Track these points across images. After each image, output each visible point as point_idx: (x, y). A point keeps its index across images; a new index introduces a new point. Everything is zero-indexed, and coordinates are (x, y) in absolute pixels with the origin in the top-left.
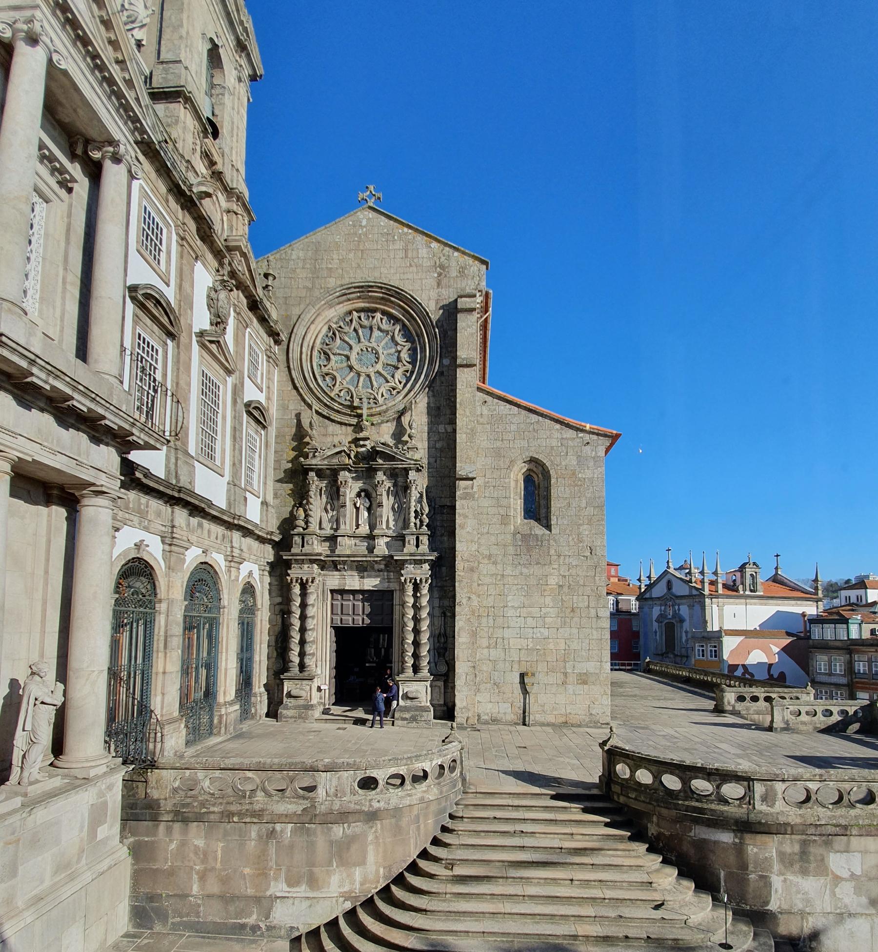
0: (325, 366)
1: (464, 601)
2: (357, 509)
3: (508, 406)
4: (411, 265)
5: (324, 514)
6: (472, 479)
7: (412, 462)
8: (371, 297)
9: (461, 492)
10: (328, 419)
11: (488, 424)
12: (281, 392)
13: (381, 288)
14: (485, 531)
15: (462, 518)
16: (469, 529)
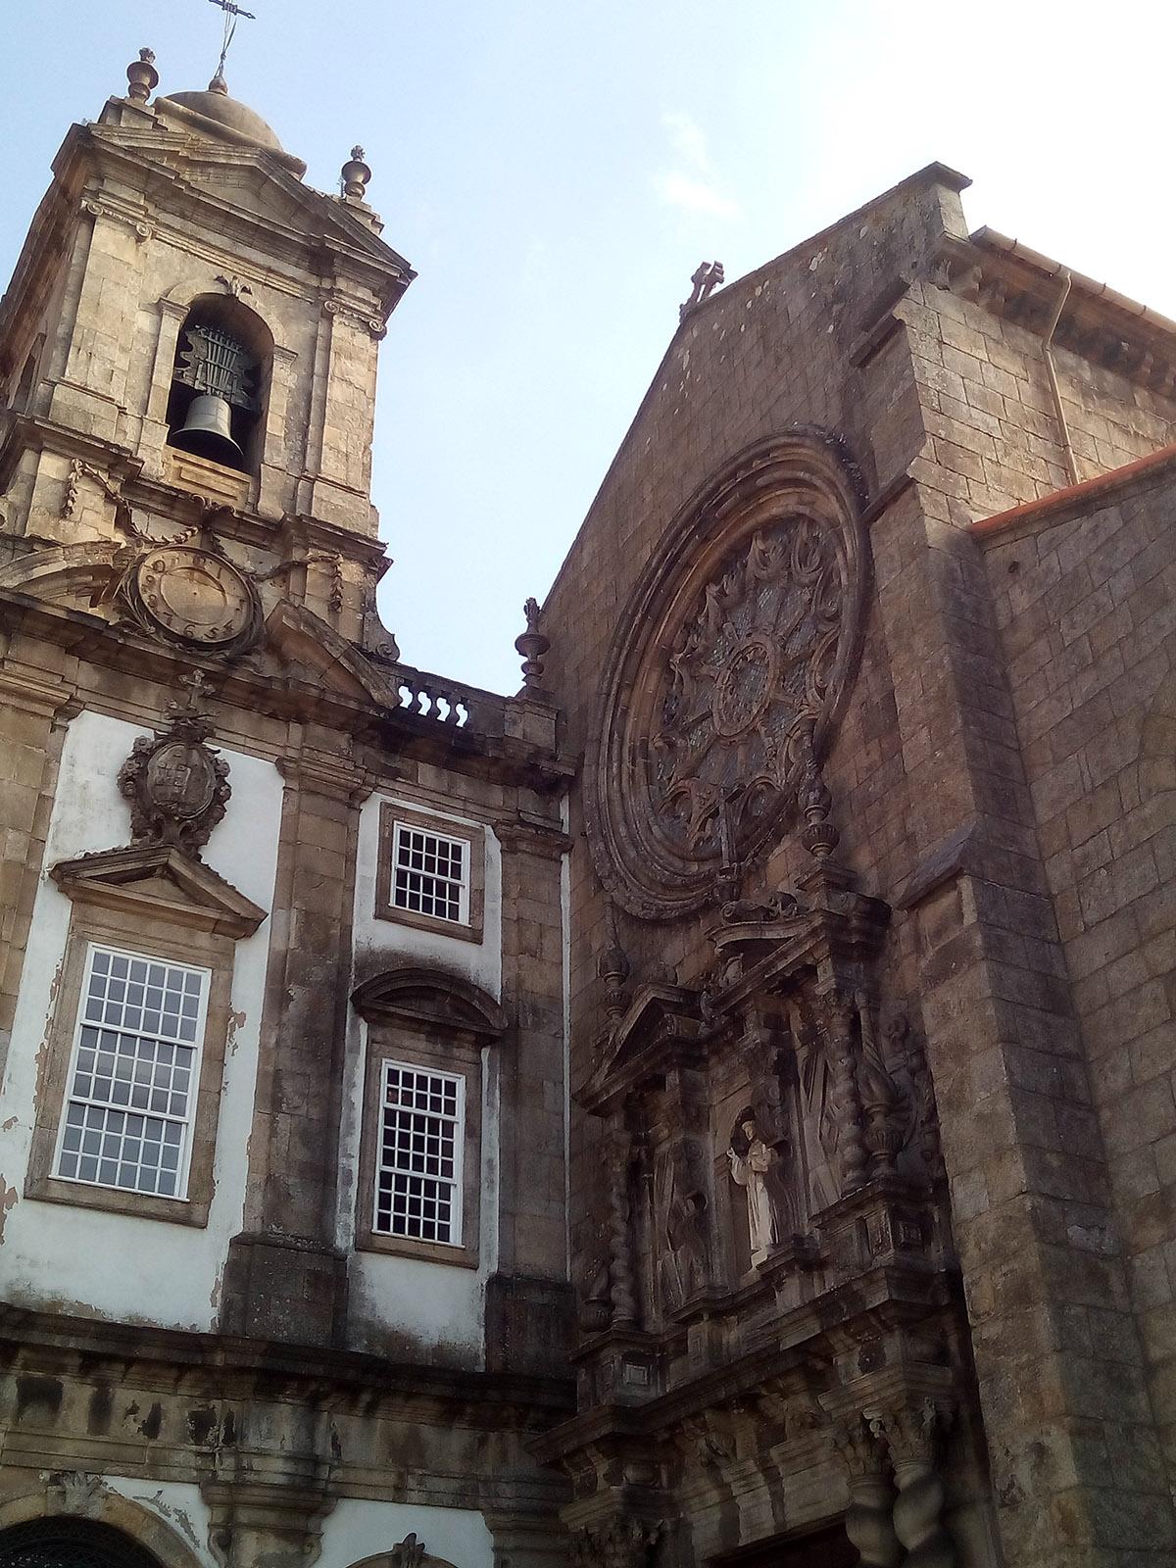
0: (670, 779)
1: (1024, 1475)
2: (743, 1189)
3: (1086, 525)
4: (778, 360)
5: (669, 1254)
6: (948, 881)
7: (803, 930)
8: (725, 517)
9: (931, 953)
10: (656, 923)
11: (1038, 635)
12: (577, 913)
13: (733, 475)
14: (1117, 1082)
15: (949, 1064)
16: (979, 1099)
